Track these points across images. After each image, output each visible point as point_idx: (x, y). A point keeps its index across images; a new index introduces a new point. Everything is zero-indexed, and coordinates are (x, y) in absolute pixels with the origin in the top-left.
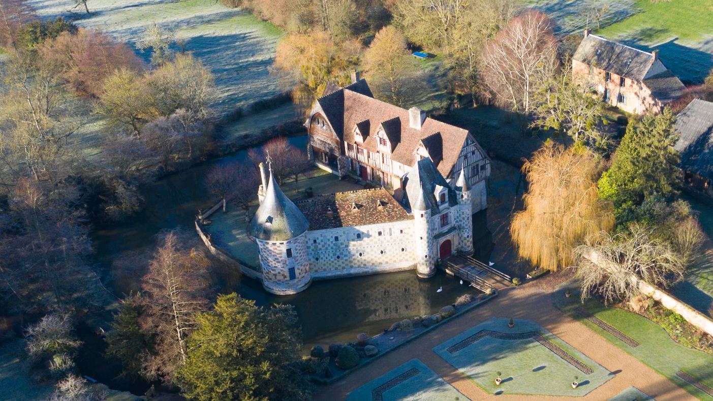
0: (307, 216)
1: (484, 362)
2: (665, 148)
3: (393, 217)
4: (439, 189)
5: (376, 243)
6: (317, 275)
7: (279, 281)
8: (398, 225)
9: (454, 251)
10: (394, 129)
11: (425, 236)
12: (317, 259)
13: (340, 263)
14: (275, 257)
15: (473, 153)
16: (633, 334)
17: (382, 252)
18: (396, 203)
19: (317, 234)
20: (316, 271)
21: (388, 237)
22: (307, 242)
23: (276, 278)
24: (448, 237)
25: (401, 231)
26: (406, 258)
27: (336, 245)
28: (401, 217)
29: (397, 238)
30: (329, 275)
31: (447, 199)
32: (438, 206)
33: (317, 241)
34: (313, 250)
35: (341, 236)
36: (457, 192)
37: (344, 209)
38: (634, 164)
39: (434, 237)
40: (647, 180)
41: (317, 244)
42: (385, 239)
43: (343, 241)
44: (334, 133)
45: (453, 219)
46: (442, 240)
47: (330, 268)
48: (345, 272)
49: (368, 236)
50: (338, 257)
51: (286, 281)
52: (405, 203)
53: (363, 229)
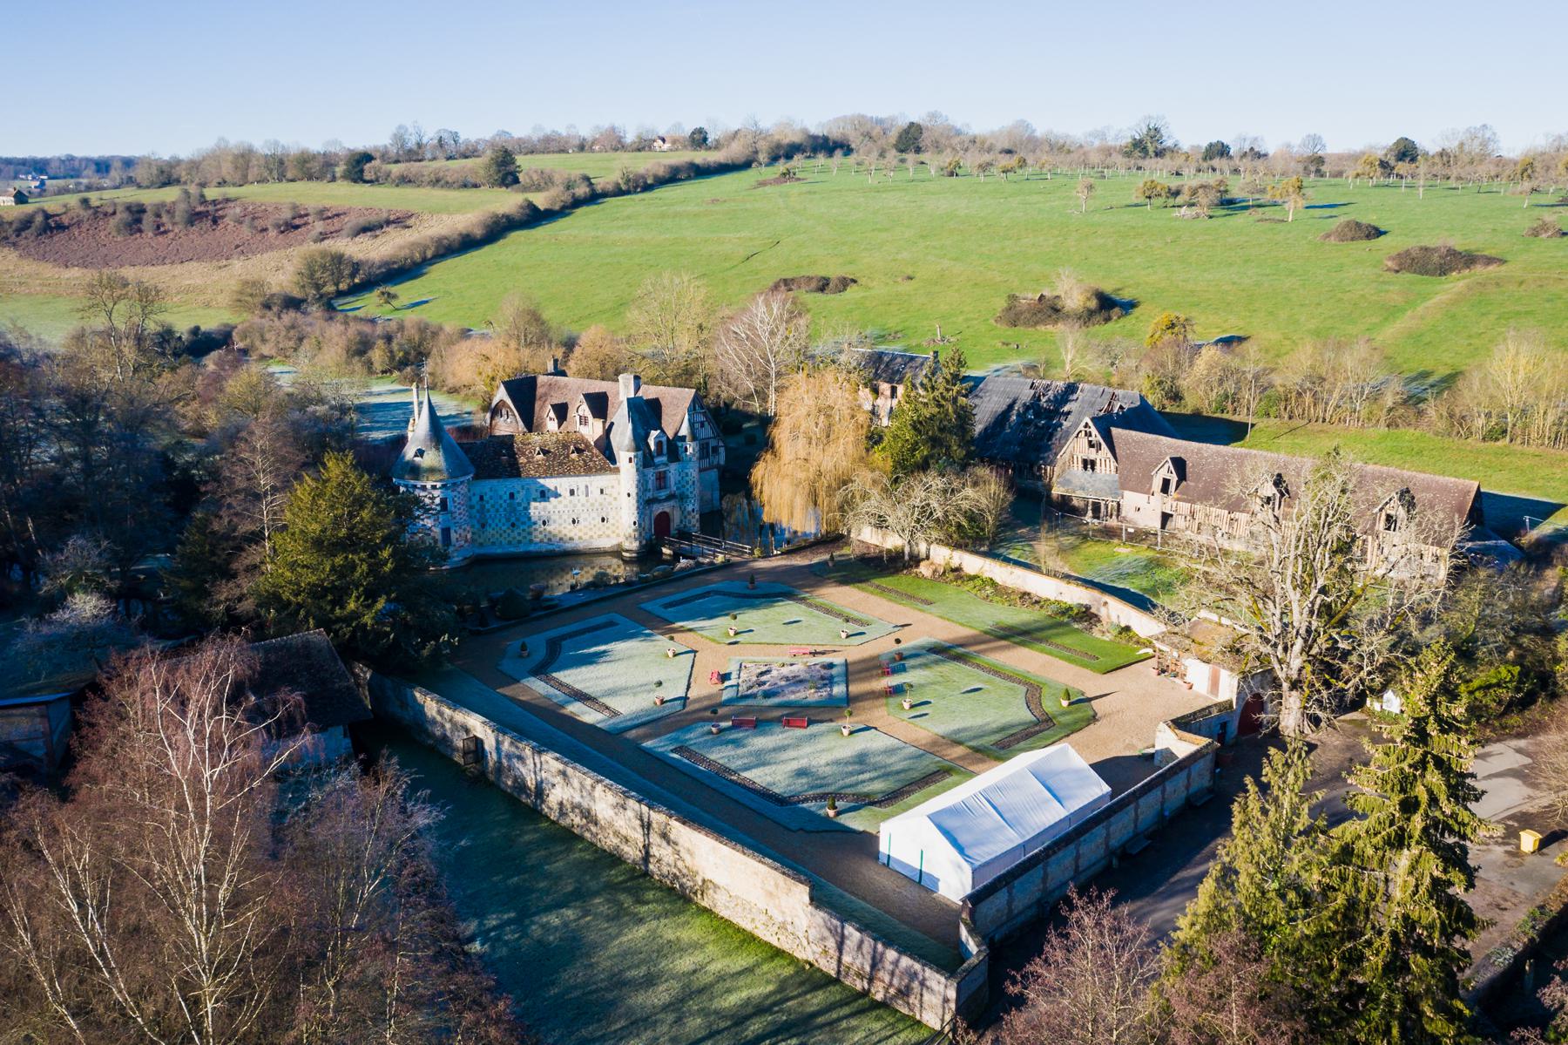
0: (473, 461)
1: (711, 617)
2: (955, 400)
3: (590, 469)
4: (654, 434)
5: (566, 506)
6: (482, 551)
8: (597, 481)
9: (673, 532)
10: (599, 404)
11: (634, 491)
12: (483, 526)
15: (702, 425)
16: (927, 595)
17: (574, 522)
18: (595, 451)
19: (487, 486)
20: (481, 544)
21: (582, 497)
22: (470, 499)
24: (665, 507)
25: (602, 492)
26: (608, 532)
28: (602, 470)
30: (499, 551)
31: (665, 450)
32: (652, 457)
36: (679, 444)
37: (524, 454)
38: (914, 428)
39: (645, 502)
40: (933, 447)
44: (521, 423)
45: (672, 483)
46: (658, 509)
47: (500, 541)
48: (522, 549)
49: (557, 495)
50: (513, 525)
52: (612, 458)
53: (550, 483)
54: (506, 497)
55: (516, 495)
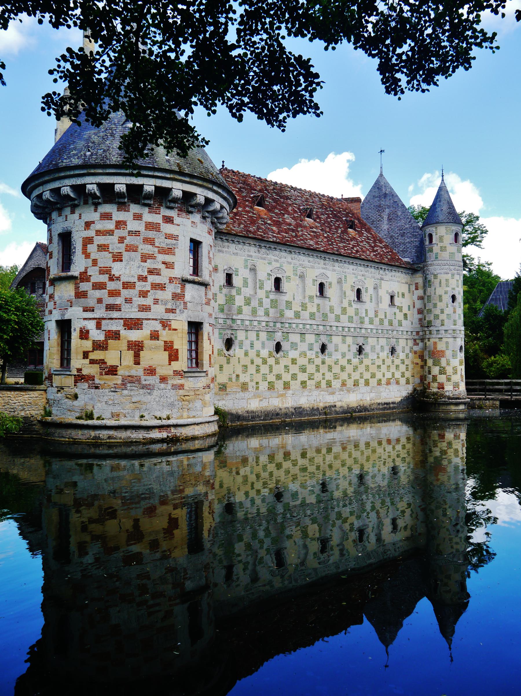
7: (151, 371)
12: (229, 343)
13: (279, 369)
14: (150, 264)
20: (223, 388)
23: (137, 363)
27: (276, 307)
29: (386, 316)
33: (236, 281)
34: (222, 310)
35: (288, 278)
41: (234, 292)
42: (366, 310)
43: (291, 299)
50: (278, 347)
51: (176, 373)
54: (270, 285)
55: (285, 286)
